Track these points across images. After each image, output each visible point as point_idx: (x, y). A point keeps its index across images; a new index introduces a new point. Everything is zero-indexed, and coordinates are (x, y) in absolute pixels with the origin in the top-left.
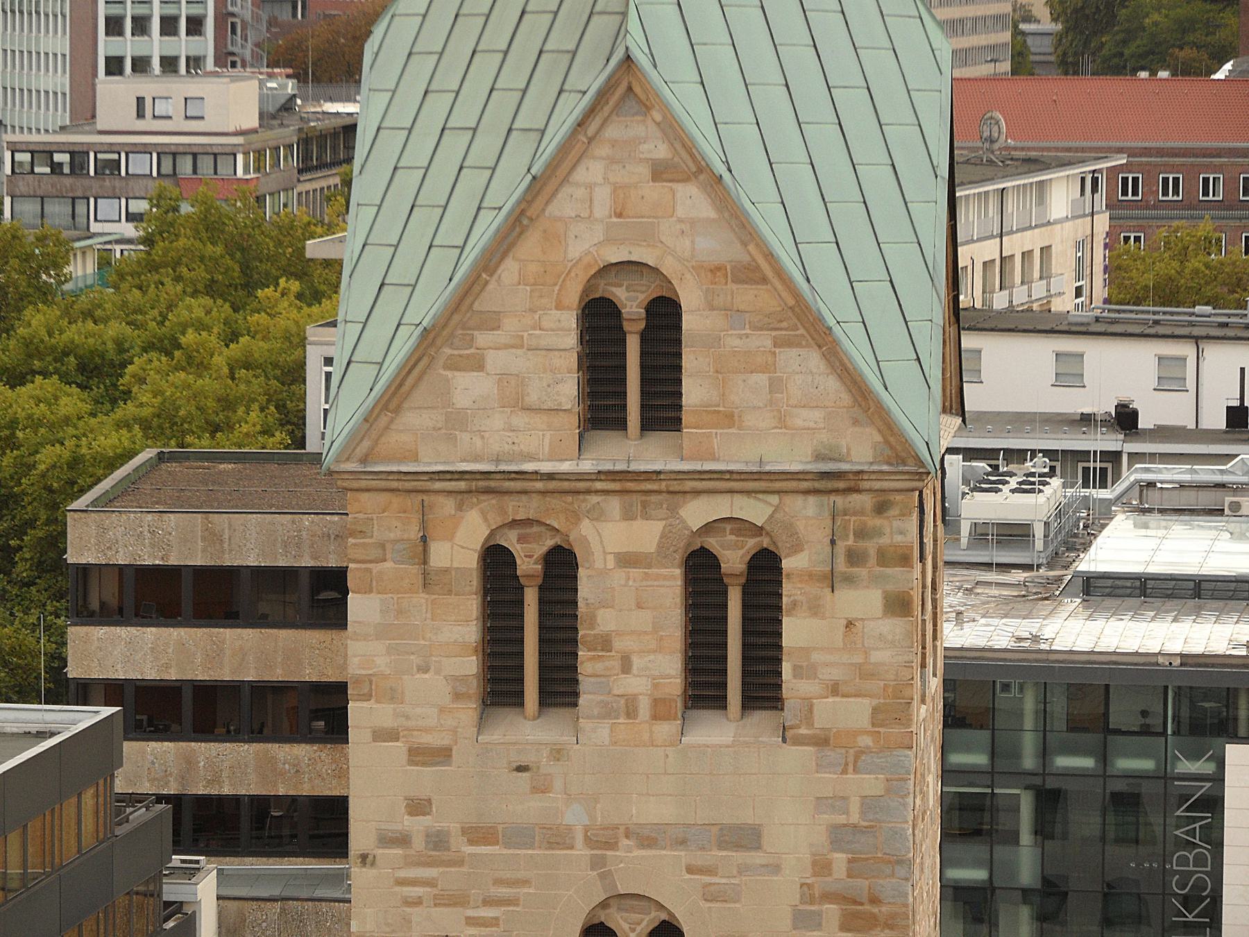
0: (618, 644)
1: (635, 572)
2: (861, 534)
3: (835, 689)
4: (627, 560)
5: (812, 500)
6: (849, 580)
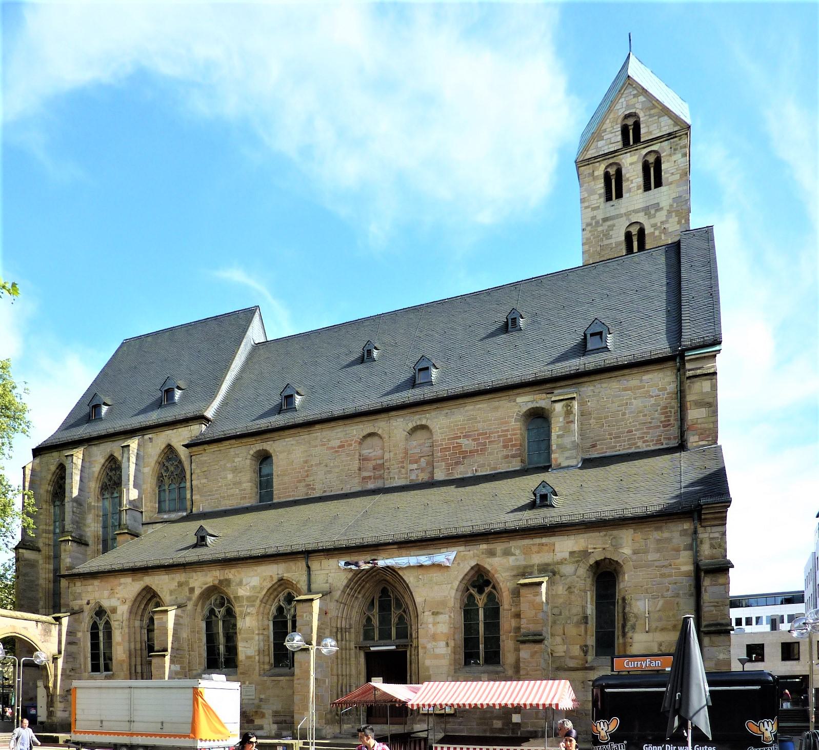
0: (630, 179)
1: (633, 166)
2: (677, 145)
3: (672, 174)
4: (631, 164)
5: (667, 142)
6: (675, 154)
